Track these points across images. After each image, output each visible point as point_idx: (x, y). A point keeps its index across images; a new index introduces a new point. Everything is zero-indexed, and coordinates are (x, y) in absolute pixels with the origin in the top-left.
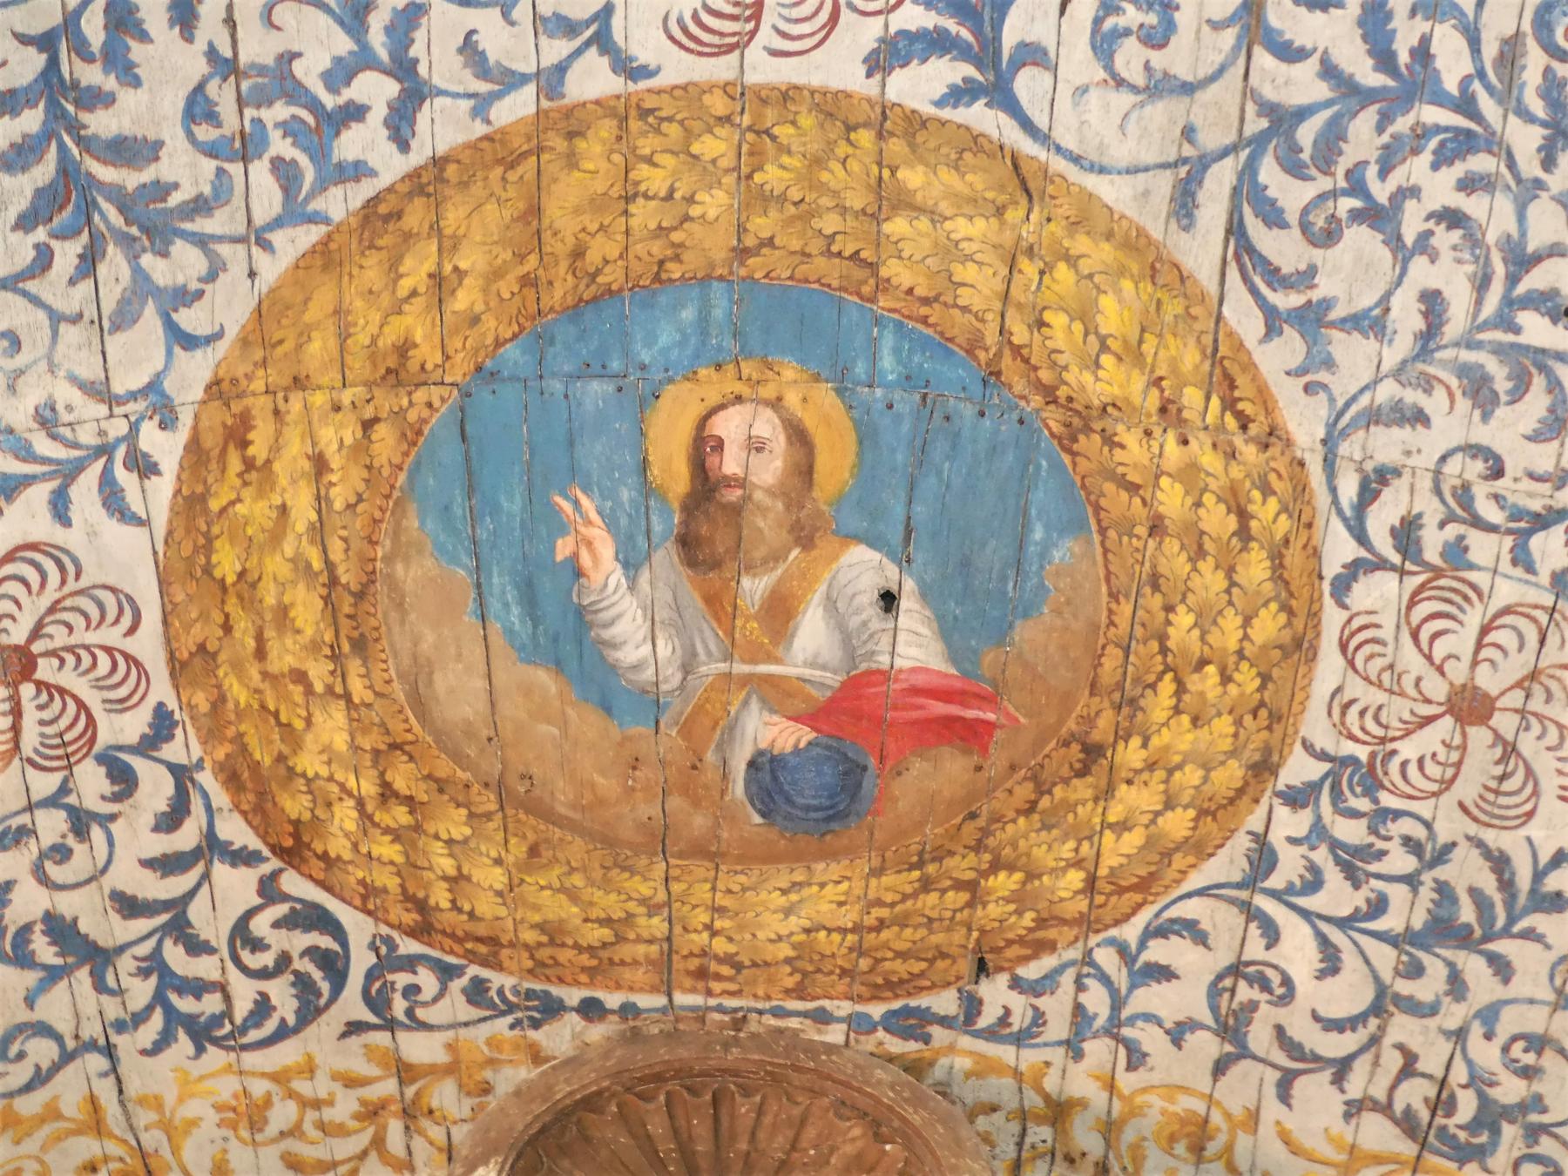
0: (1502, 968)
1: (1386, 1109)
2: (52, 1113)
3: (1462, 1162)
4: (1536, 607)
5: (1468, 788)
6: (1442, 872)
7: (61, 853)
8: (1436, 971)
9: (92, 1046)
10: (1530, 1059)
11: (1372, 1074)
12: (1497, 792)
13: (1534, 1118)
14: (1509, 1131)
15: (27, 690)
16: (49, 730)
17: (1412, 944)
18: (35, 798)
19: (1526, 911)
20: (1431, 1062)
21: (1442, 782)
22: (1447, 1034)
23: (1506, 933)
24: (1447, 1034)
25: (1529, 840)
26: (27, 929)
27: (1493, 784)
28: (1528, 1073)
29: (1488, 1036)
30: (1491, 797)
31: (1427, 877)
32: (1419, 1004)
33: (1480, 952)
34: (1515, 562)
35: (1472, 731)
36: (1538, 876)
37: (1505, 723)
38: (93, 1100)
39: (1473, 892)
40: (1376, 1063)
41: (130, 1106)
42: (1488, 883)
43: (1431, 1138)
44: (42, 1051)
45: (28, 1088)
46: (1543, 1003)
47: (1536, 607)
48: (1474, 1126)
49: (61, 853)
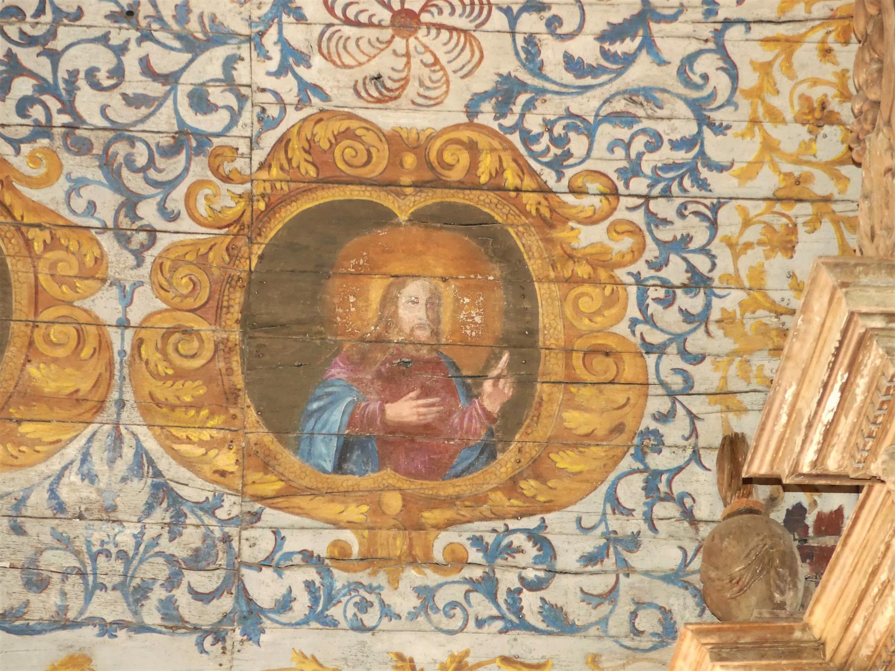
2: (765, 69)
7: (554, 23)
9: (719, 35)
15: (425, 17)
16: (459, 10)
18: (507, 28)
26: (604, 53)
38: (766, 40)
41: (783, 19)
44: (707, 64)
45: (734, 78)
49: (554, 23)
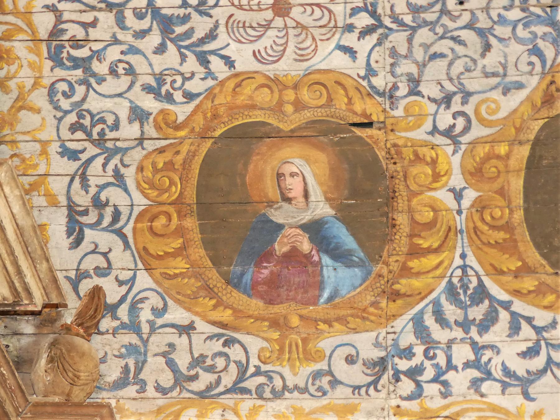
0: (161, 49)
1: (59, 20)
3: (50, 58)
4: (335, 21)
5: (240, 15)
6: (195, 16)
8: (145, 24)
10: (121, 71)
11: (75, 11)
12: (244, 27)
13: (92, 81)
14: (79, 72)
17: (152, 12)
19: (194, 53)
20: (93, 33)
21: (241, 6)
22: (114, 36)
23: (179, 48)
24: (114, 36)
25: (228, 45)
27: (247, 24)
28: (113, 72)
29: (122, 53)
30: (241, 25)
31: (189, 10)
32: (123, 22)
33: (163, 39)
34: (352, 9)
35: (270, 12)
36: (213, 52)
37: (279, 22)
39: (192, 29)
40: (81, 12)
42: (199, 34)
43: (54, 43)
46: (153, 69)
47: (335, 21)
48: (70, 58)
